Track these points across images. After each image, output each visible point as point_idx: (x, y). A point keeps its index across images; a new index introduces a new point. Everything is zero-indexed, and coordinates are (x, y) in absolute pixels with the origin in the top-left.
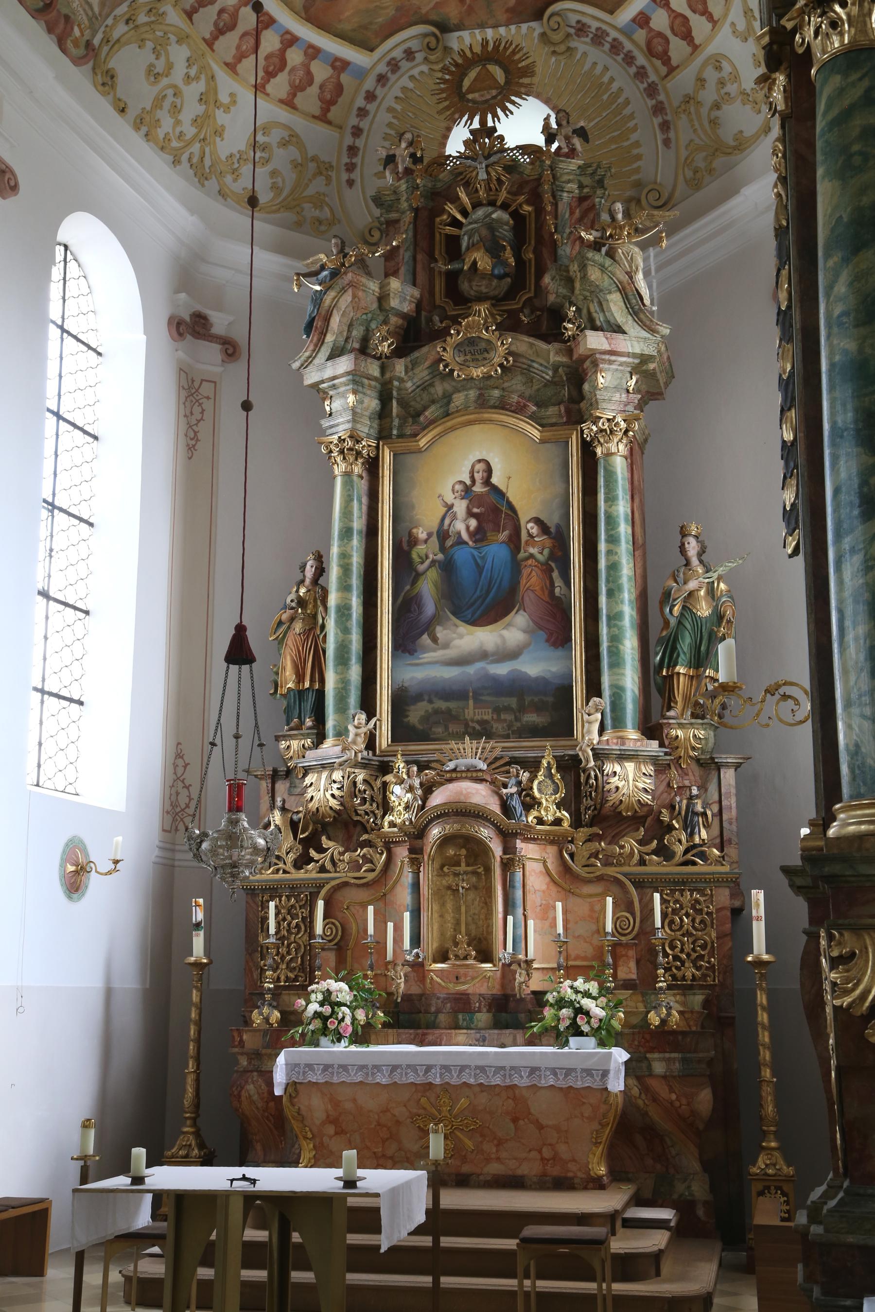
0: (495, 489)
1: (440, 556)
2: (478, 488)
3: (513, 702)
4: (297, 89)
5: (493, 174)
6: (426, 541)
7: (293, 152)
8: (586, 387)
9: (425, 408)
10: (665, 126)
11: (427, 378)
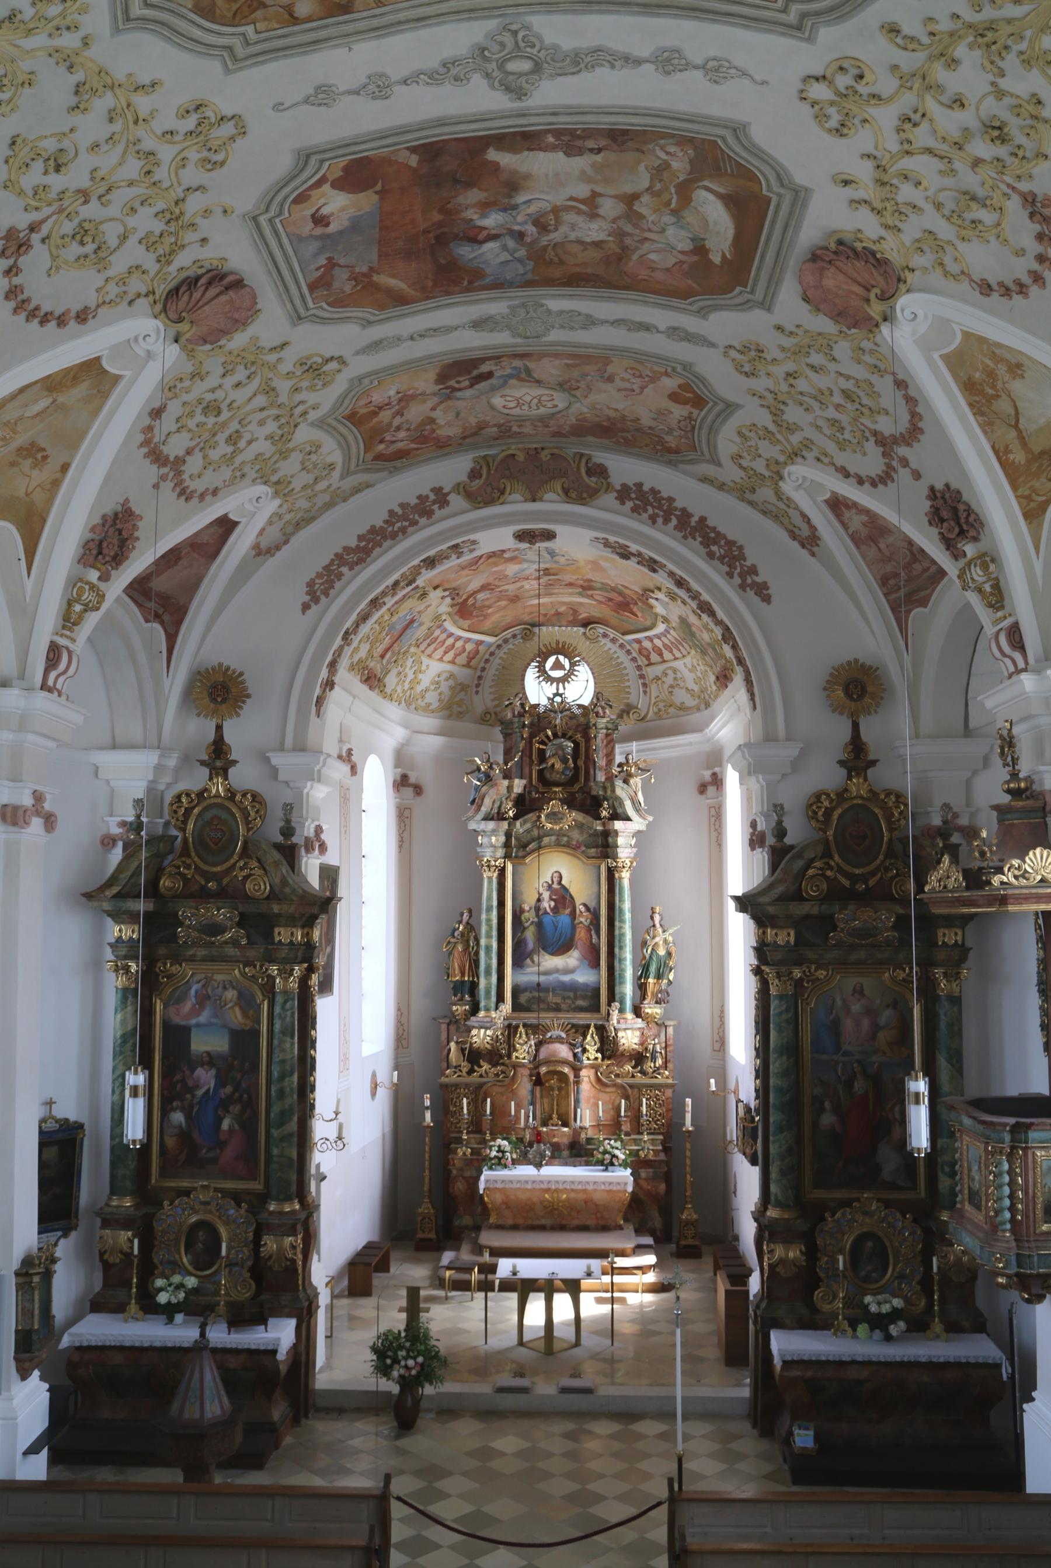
0: (564, 887)
1: (536, 920)
2: (555, 886)
3: (571, 994)
4: (456, 655)
7: (451, 682)
8: (610, 840)
9: (529, 843)
10: (645, 685)
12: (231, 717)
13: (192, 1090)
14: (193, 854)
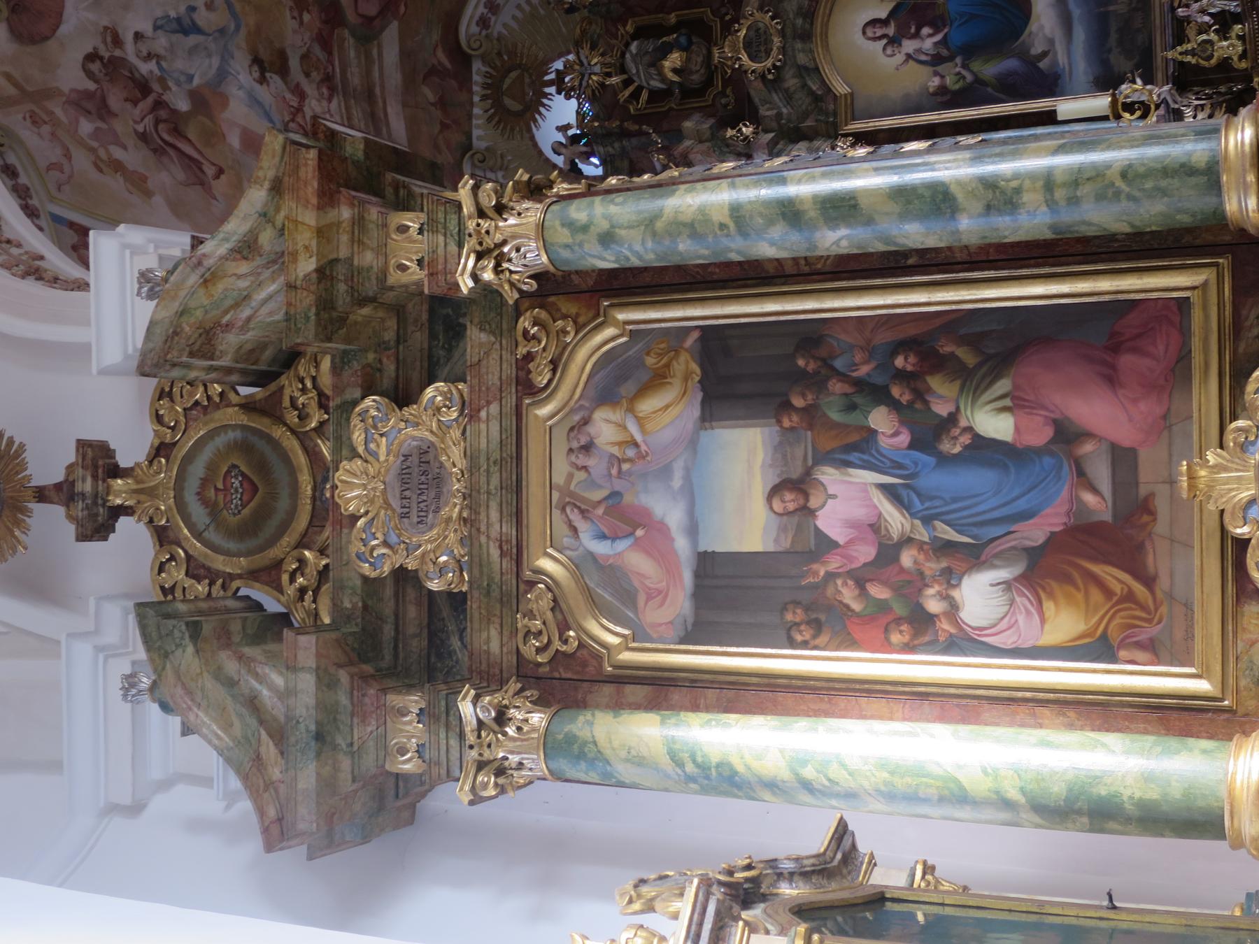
0: (892, 14)
1: (958, 60)
2: (891, 31)
5: (595, 60)
6: (942, 77)
11: (781, 95)
12: (23, 466)
13: (888, 552)
14: (275, 552)
